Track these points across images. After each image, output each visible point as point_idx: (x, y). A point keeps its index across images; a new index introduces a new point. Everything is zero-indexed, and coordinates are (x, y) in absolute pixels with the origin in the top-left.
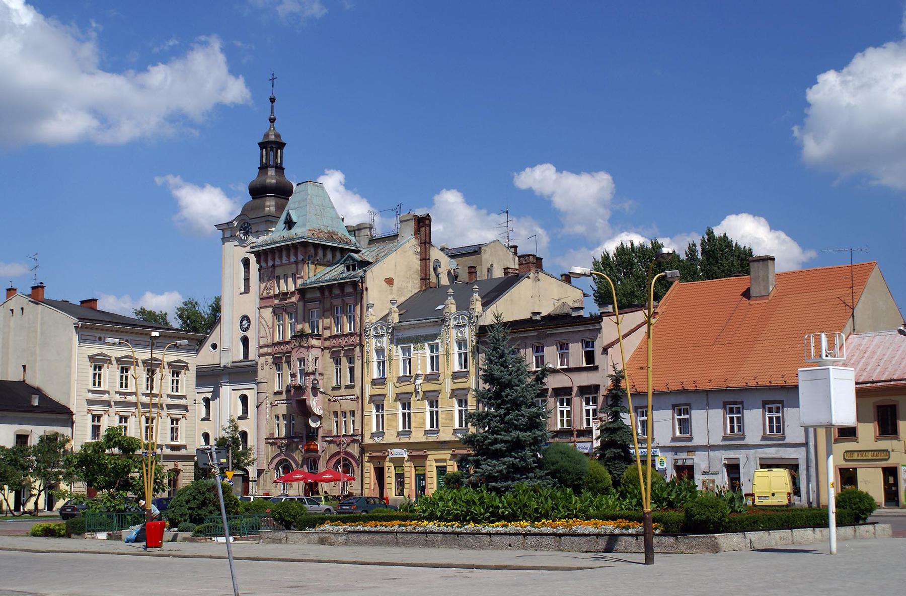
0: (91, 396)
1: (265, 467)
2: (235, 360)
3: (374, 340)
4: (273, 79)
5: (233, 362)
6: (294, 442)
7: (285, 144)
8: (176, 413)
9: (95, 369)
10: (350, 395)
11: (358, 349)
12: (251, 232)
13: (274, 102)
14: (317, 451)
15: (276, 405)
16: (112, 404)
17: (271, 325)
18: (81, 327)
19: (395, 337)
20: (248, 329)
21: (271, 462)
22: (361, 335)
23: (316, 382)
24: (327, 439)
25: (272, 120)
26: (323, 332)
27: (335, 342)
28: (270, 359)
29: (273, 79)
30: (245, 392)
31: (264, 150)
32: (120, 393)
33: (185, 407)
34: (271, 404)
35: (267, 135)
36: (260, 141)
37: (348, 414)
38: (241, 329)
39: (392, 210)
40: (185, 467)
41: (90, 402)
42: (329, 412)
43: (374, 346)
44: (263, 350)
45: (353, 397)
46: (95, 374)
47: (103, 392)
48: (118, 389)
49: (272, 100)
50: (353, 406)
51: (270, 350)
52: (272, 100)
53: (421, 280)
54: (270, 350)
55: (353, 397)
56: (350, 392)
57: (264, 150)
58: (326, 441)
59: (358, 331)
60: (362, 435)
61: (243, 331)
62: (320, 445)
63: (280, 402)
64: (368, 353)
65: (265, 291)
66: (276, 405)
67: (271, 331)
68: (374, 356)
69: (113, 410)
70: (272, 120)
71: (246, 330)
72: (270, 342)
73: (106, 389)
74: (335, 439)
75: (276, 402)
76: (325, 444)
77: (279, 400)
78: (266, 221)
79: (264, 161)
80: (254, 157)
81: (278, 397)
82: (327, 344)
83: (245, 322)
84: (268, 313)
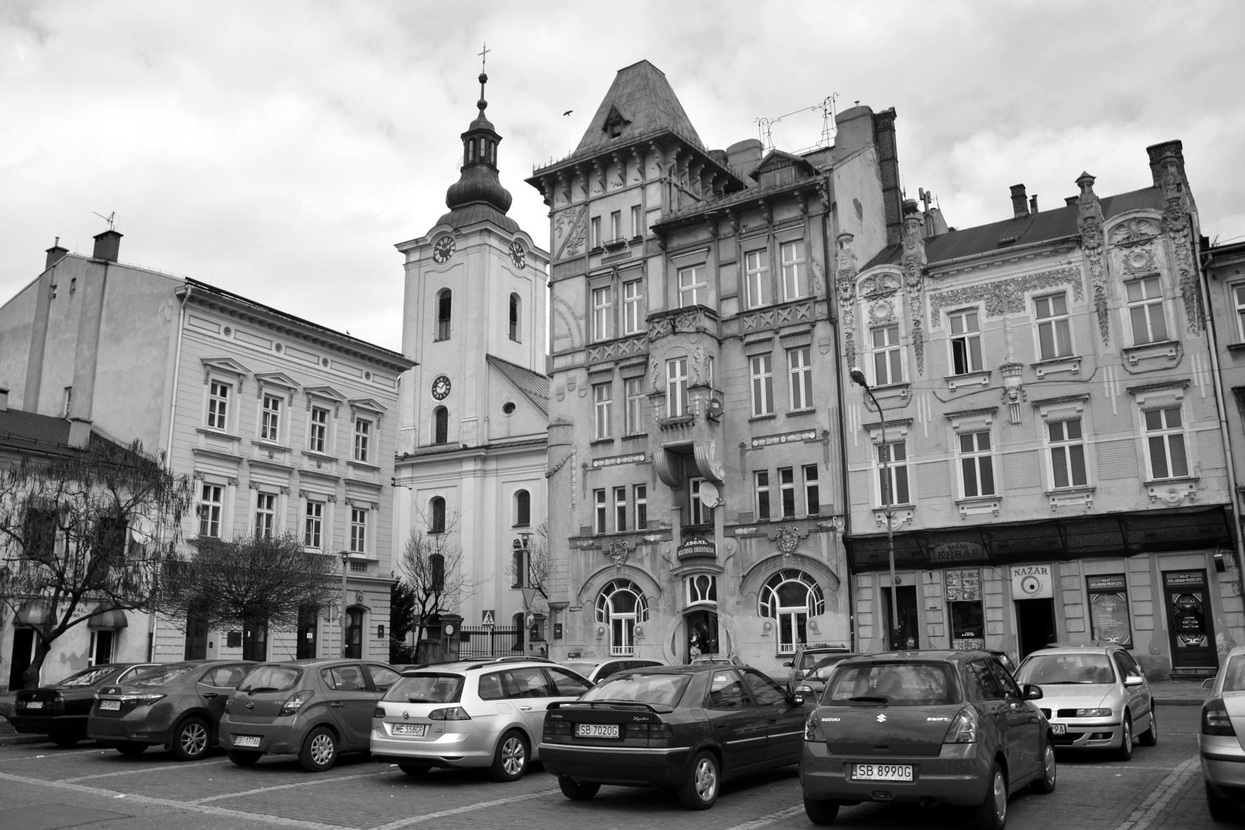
0: (204, 443)
1: (571, 597)
2: (423, 443)
3: (865, 306)
4: (484, 53)
5: (419, 447)
6: (646, 543)
7: (500, 138)
8: (363, 498)
9: (214, 391)
10: (802, 432)
11: (823, 331)
12: (454, 250)
13: (485, 82)
14: (713, 557)
15: (599, 468)
16: (245, 463)
17: (581, 310)
18: (191, 299)
19: (928, 294)
20: (447, 395)
21: (585, 588)
22: (828, 300)
23: (716, 406)
24: (739, 531)
25: (482, 105)
26: (719, 307)
27: (750, 322)
28: (580, 376)
29: (484, 53)
30: (441, 494)
31: (471, 143)
32: (262, 446)
33: (378, 488)
34: (584, 466)
35: (473, 124)
36: (466, 129)
37: (798, 474)
38: (435, 396)
39: (814, 108)
40: (377, 603)
41: (200, 453)
42: (744, 472)
43: (866, 318)
44: (560, 363)
45: (812, 435)
46: (213, 403)
47: (231, 439)
48: (257, 437)
49: (483, 79)
50: (813, 455)
51: (580, 358)
52: (483, 79)
53: (888, 226)
54: (580, 358)
55: (812, 435)
56: (802, 423)
57: (471, 143)
58: (734, 536)
59: (820, 293)
60: (846, 516)
61: (439, 399)
62: (721, 543)
63: (607, 462)
64: (849, 335)
65: (566, 250)
66: (599, 468)
67: (583, 323)
68: (867, 339)
69: (244, 475)
70: (482, 105)
71: (443, 398)
72: (578, 342)
73: (235, 433)
74: (763, 529)
75: (596, 464)
76: (732, 543)
77: (603, 459)
78: (481, 231)
79: (471, 157)
80: (456, 154)
81: (601, 451)
82: (733, 329)
83: (441, 389)
84: (574, 289)
